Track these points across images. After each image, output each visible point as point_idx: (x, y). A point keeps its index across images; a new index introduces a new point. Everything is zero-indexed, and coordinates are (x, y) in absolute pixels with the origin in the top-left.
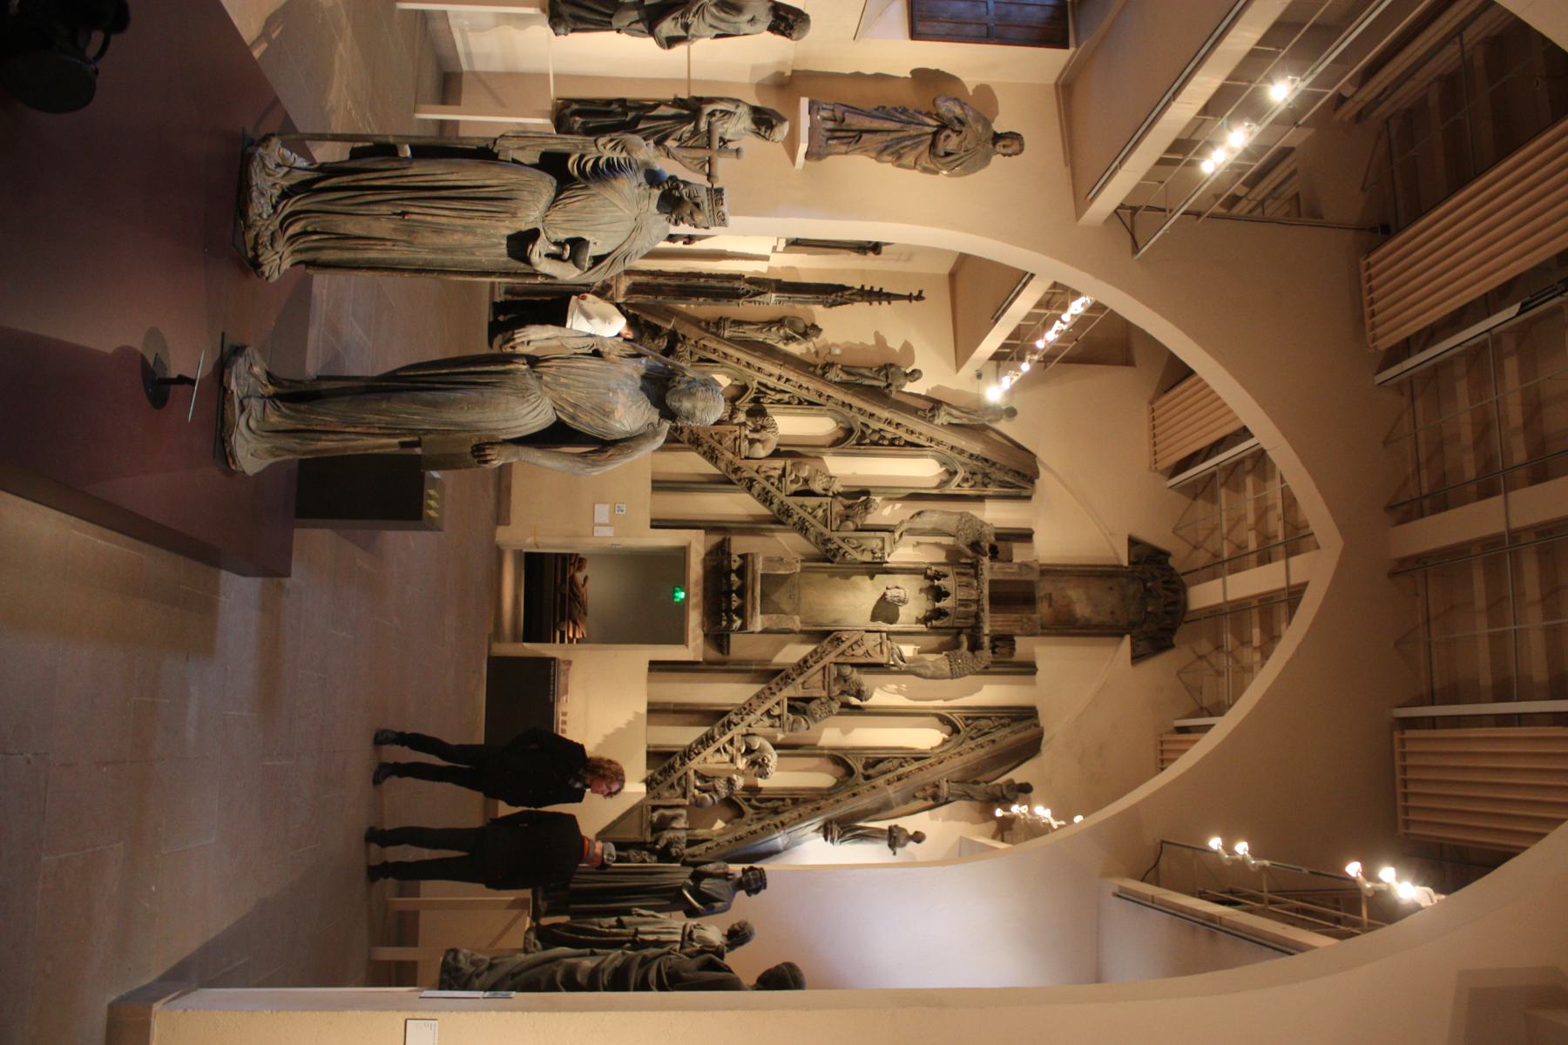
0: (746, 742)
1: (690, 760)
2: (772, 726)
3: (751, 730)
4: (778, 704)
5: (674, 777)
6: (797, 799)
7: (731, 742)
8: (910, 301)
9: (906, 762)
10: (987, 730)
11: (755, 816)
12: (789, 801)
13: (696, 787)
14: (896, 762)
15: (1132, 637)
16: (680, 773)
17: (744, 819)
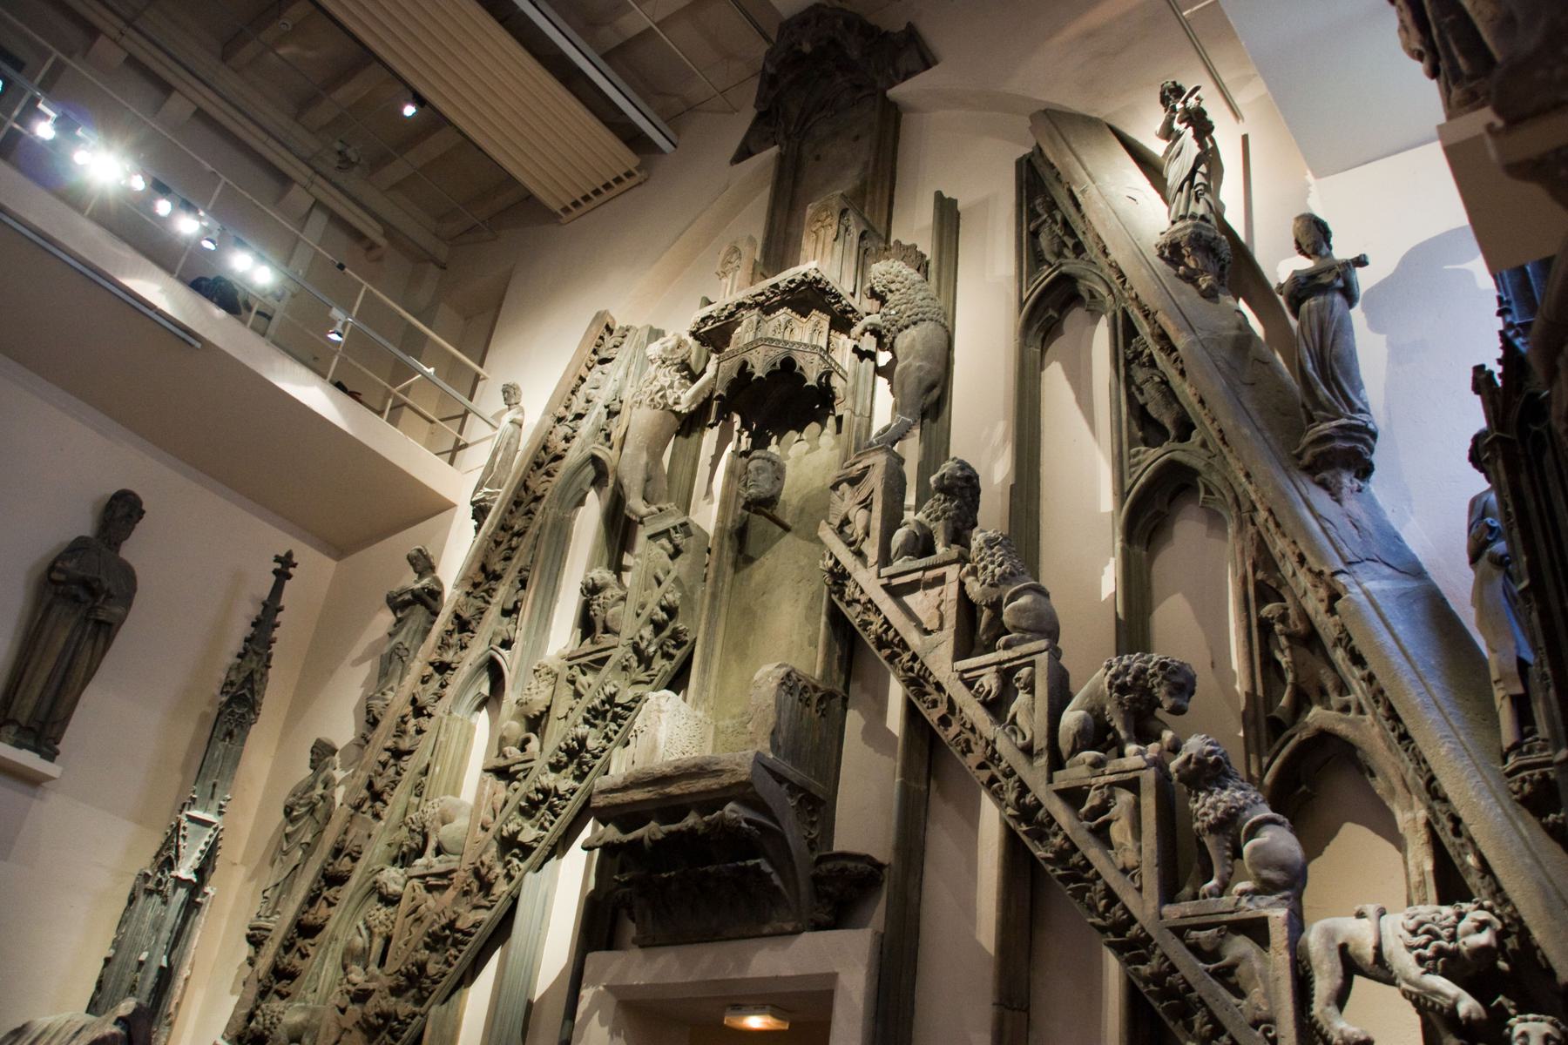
0: (1074, 751)
1: (1132, 920)
2: (1030, 687)
3: (1041, 742)
4: (969, 684)
5: (1192, 969)
6: (1259, 585)
7: (1073, 796)
8: (289, 577)
9: (1138, 355)
10: (1057, 229)
11: (1335, 700)
12: (1270, 609)
13: (1224, 888)
14: (1140, 375)
15: (892, 85)
16: (1175, 949)
17: (1342, 728)
